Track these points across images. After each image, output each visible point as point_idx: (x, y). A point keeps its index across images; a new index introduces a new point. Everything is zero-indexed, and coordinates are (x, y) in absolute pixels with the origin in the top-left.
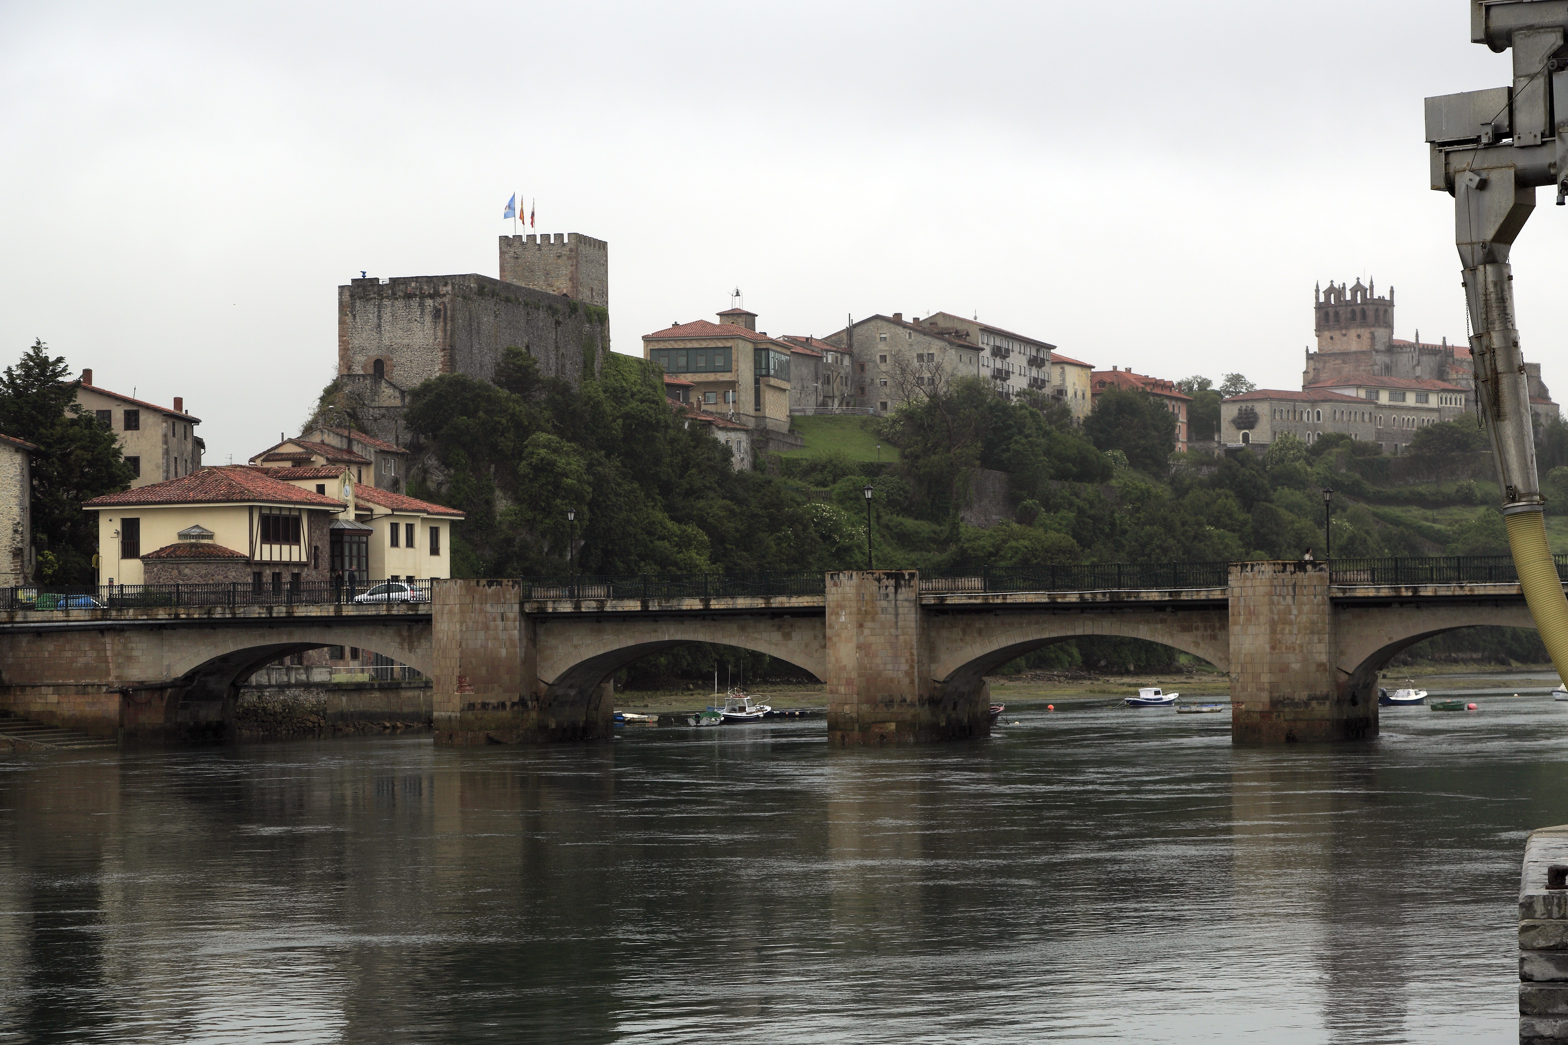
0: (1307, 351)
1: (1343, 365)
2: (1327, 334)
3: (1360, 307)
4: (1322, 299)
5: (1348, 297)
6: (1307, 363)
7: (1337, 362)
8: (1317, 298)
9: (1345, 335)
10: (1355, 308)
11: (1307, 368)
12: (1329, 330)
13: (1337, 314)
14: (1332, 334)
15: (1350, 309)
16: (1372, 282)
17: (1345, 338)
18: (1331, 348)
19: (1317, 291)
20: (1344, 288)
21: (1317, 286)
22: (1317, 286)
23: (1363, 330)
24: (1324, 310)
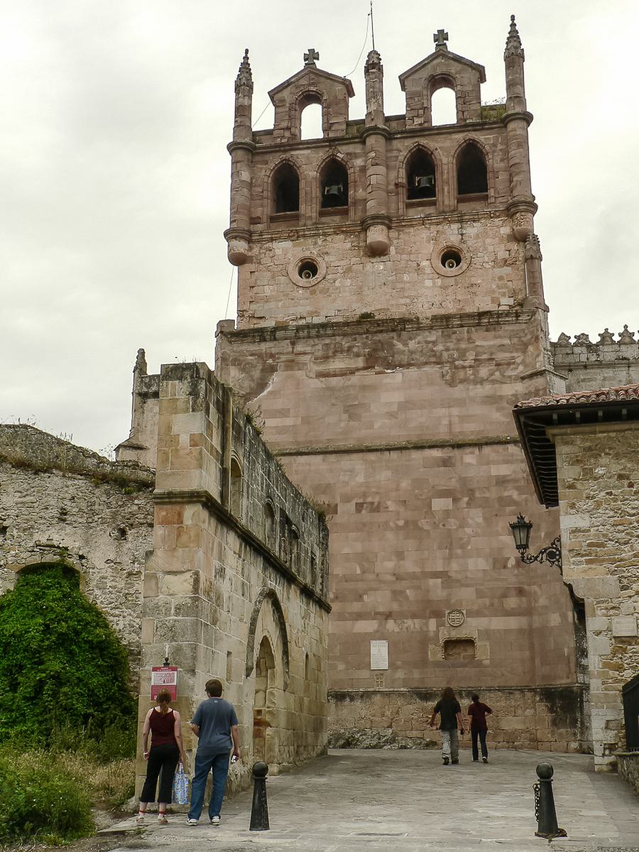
0: (141, 366)
1: (370, 377)
2: (287, 252)
3: (460, 137)
4: (263, 117)
5: (395, 103)
6: (138, 409)
7: (338, 364)
8: (243, 112)
9: (377, 251)
10: (428, 143)
11: (136, 429)
12: (295, 236)
13: (335, 174)
14: (308, 249)
15: (403, 148)
16: (514, 36)
17: (378, 265)
18: (302, 310)
19: (244, 85)
20: (374, 67)
21: (245, 68)
22: (245, 68)
23: (472, 230)
24: (275, 160)
